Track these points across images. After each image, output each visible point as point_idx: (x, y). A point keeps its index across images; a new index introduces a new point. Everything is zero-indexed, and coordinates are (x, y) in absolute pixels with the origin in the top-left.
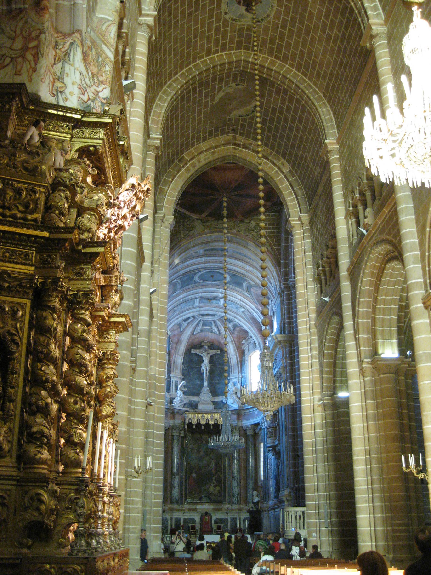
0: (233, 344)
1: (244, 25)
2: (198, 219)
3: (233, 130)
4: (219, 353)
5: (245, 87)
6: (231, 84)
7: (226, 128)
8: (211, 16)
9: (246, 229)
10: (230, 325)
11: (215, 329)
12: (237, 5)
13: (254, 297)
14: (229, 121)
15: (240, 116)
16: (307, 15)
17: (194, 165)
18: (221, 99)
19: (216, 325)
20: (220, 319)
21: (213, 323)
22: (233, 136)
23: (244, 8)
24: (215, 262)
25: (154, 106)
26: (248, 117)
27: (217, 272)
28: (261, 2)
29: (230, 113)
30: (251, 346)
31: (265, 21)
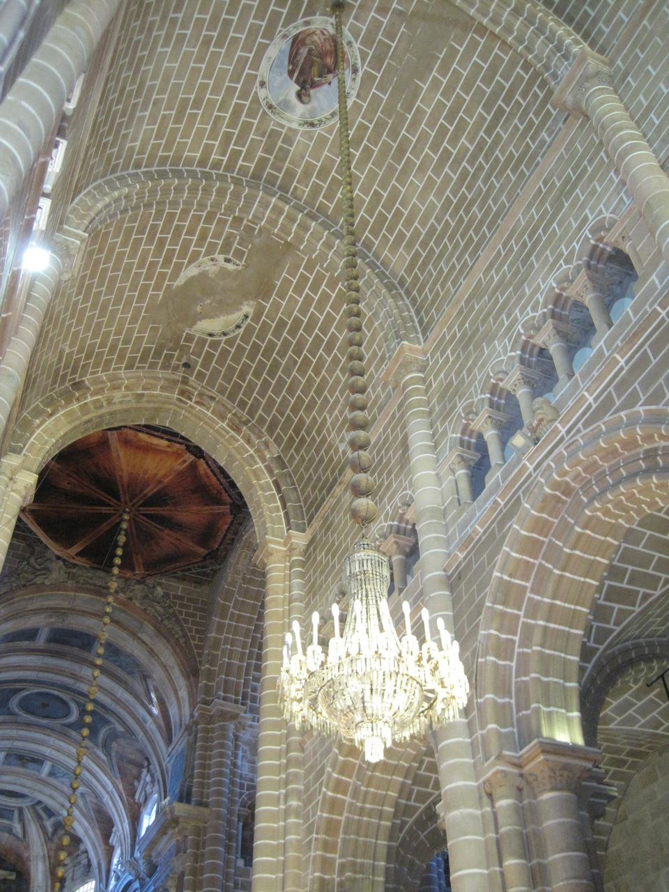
0: (44, 861)
1: (282, 126)
2: (58, 558)
3: (186, 365)
4: (13, 877)
5: (240, 268)
6: (216, 256)
7: (176, 354)
8: (236, 78)
9: (146, 597)
10: (49, 824)
11: (17, 828)
12: (286, 75)
13: (114, 760)
14: (186, 340)
15: (211, 335)
16: (410, 117)
17: (98, 405)
18: (190, 282)
19: (22, 820)
20: (33, 807)
21: (16, 815)
22: (183, 377)
23: (297, 88)
24: (59, 672)
25: (83, 193)
26: (224, 338)
27: (57, 698)
28: (330, 84)
29: (194, 323)
30: (79, 871)
31: (323, 126)
